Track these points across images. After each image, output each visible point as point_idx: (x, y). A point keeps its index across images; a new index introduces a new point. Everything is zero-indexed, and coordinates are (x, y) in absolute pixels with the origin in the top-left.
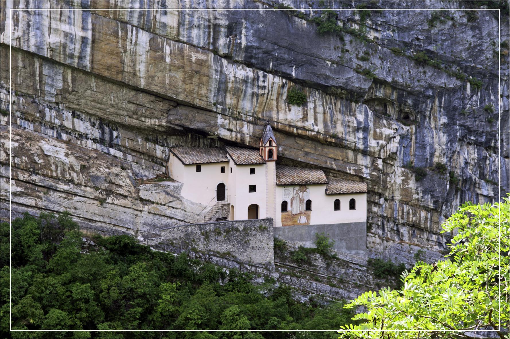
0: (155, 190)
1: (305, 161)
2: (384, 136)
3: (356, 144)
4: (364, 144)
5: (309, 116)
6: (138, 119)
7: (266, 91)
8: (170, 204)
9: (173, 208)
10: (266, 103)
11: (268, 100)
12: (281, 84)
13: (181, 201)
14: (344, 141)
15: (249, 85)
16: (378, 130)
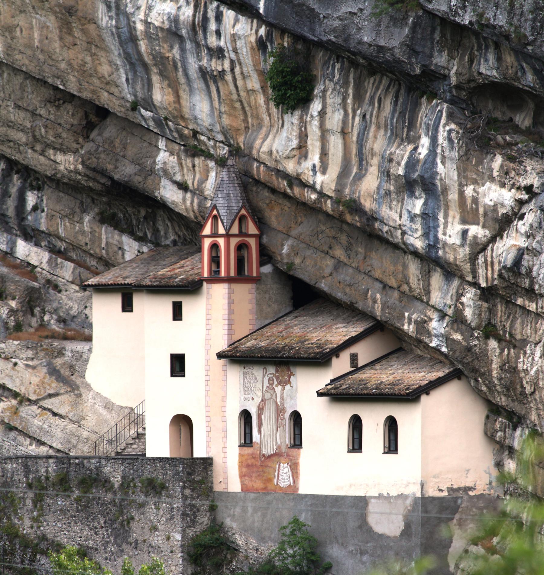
0: (28, 359)
1: (328, 292)
2: (481, 210)
3: (404, 233)
4: (426, 235)
5: (309, 142)
6: (42, 153)
7: (227, 65)
8: (47, 403)
9: (55, 414)
10: (241, 101)
11: (242, 93)
12: (253, 39)
13: (80, 395)
14: (377, 225)
15: (189, 45)
16: (469, 191)
